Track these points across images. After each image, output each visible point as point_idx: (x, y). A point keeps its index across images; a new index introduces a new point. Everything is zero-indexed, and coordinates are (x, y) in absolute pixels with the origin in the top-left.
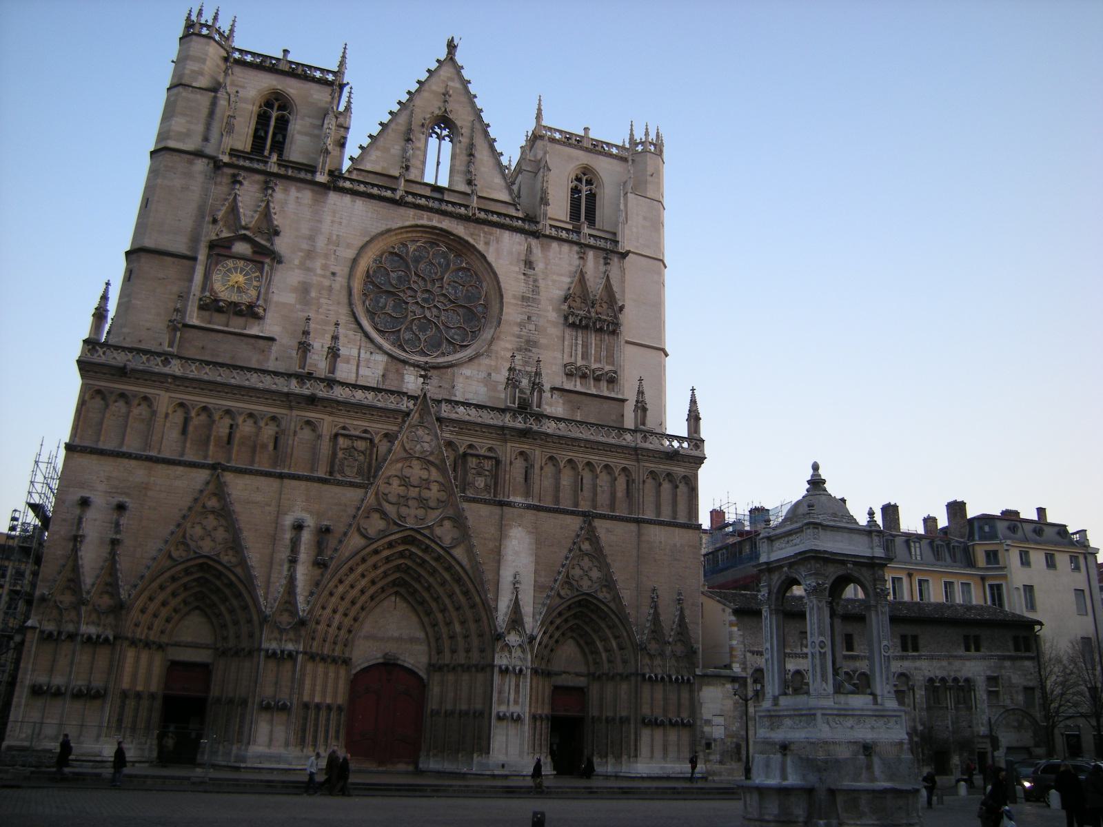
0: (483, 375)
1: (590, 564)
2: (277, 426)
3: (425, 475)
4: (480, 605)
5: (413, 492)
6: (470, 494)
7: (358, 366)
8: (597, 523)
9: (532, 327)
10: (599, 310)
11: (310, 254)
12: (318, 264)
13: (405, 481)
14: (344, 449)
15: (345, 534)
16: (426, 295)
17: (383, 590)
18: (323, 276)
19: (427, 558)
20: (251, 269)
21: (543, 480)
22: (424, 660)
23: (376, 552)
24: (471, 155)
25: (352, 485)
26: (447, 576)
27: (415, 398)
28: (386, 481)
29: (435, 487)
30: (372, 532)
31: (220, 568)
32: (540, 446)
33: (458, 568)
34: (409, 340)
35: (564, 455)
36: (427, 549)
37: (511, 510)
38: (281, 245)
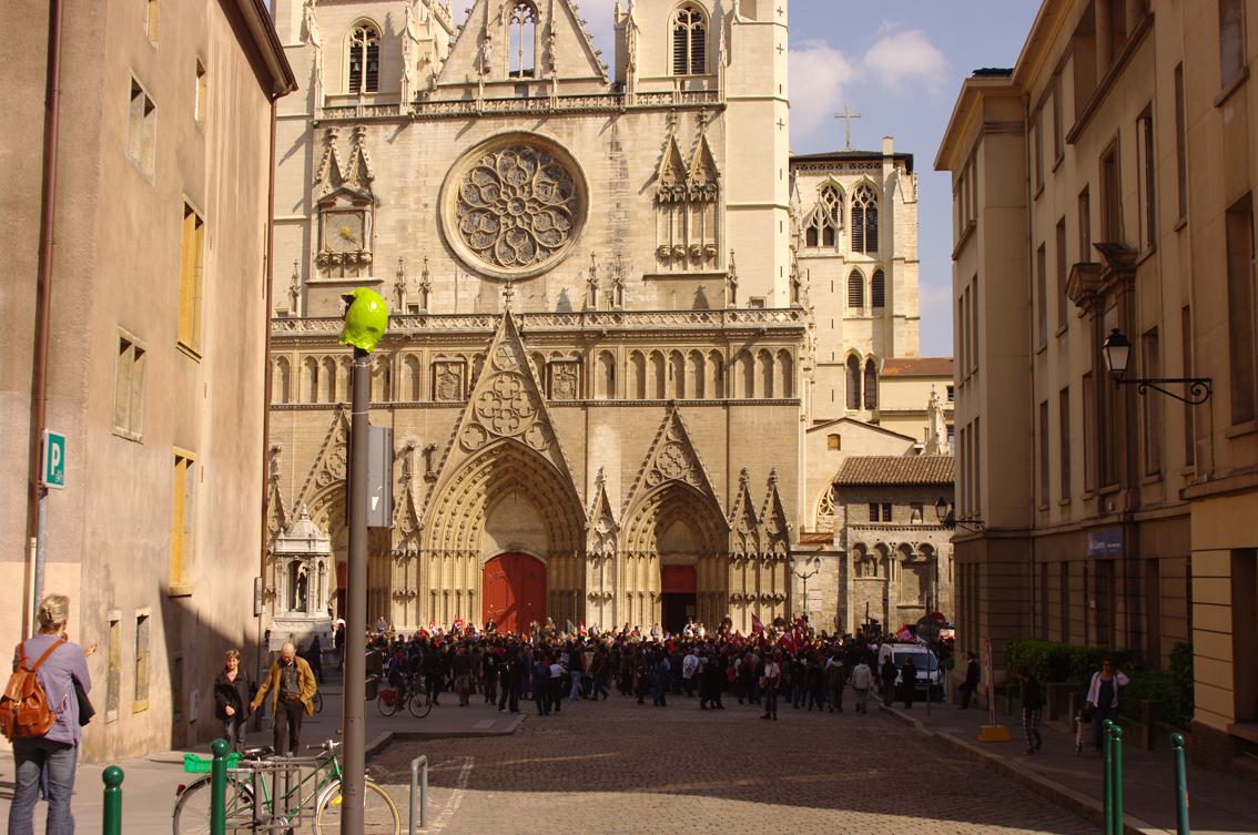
0: (574, 276)
1: (679, 452)
5: (506, 405)
7: (456, 291)
8: (682, 412)
9: (622, 215)
11: (403, 192)
12: (410, 200)
13: (497, 395)
15: (448, 450)
16: (516, 204)
17: (500, 490)
18: (417, 210)
22: (544, 548)
23: (479, 461)
24: (549, 33)
29: (524, 397)
30: (473, 446)
35: (647, 350)
37: (596, 409)
38: (378, 188)
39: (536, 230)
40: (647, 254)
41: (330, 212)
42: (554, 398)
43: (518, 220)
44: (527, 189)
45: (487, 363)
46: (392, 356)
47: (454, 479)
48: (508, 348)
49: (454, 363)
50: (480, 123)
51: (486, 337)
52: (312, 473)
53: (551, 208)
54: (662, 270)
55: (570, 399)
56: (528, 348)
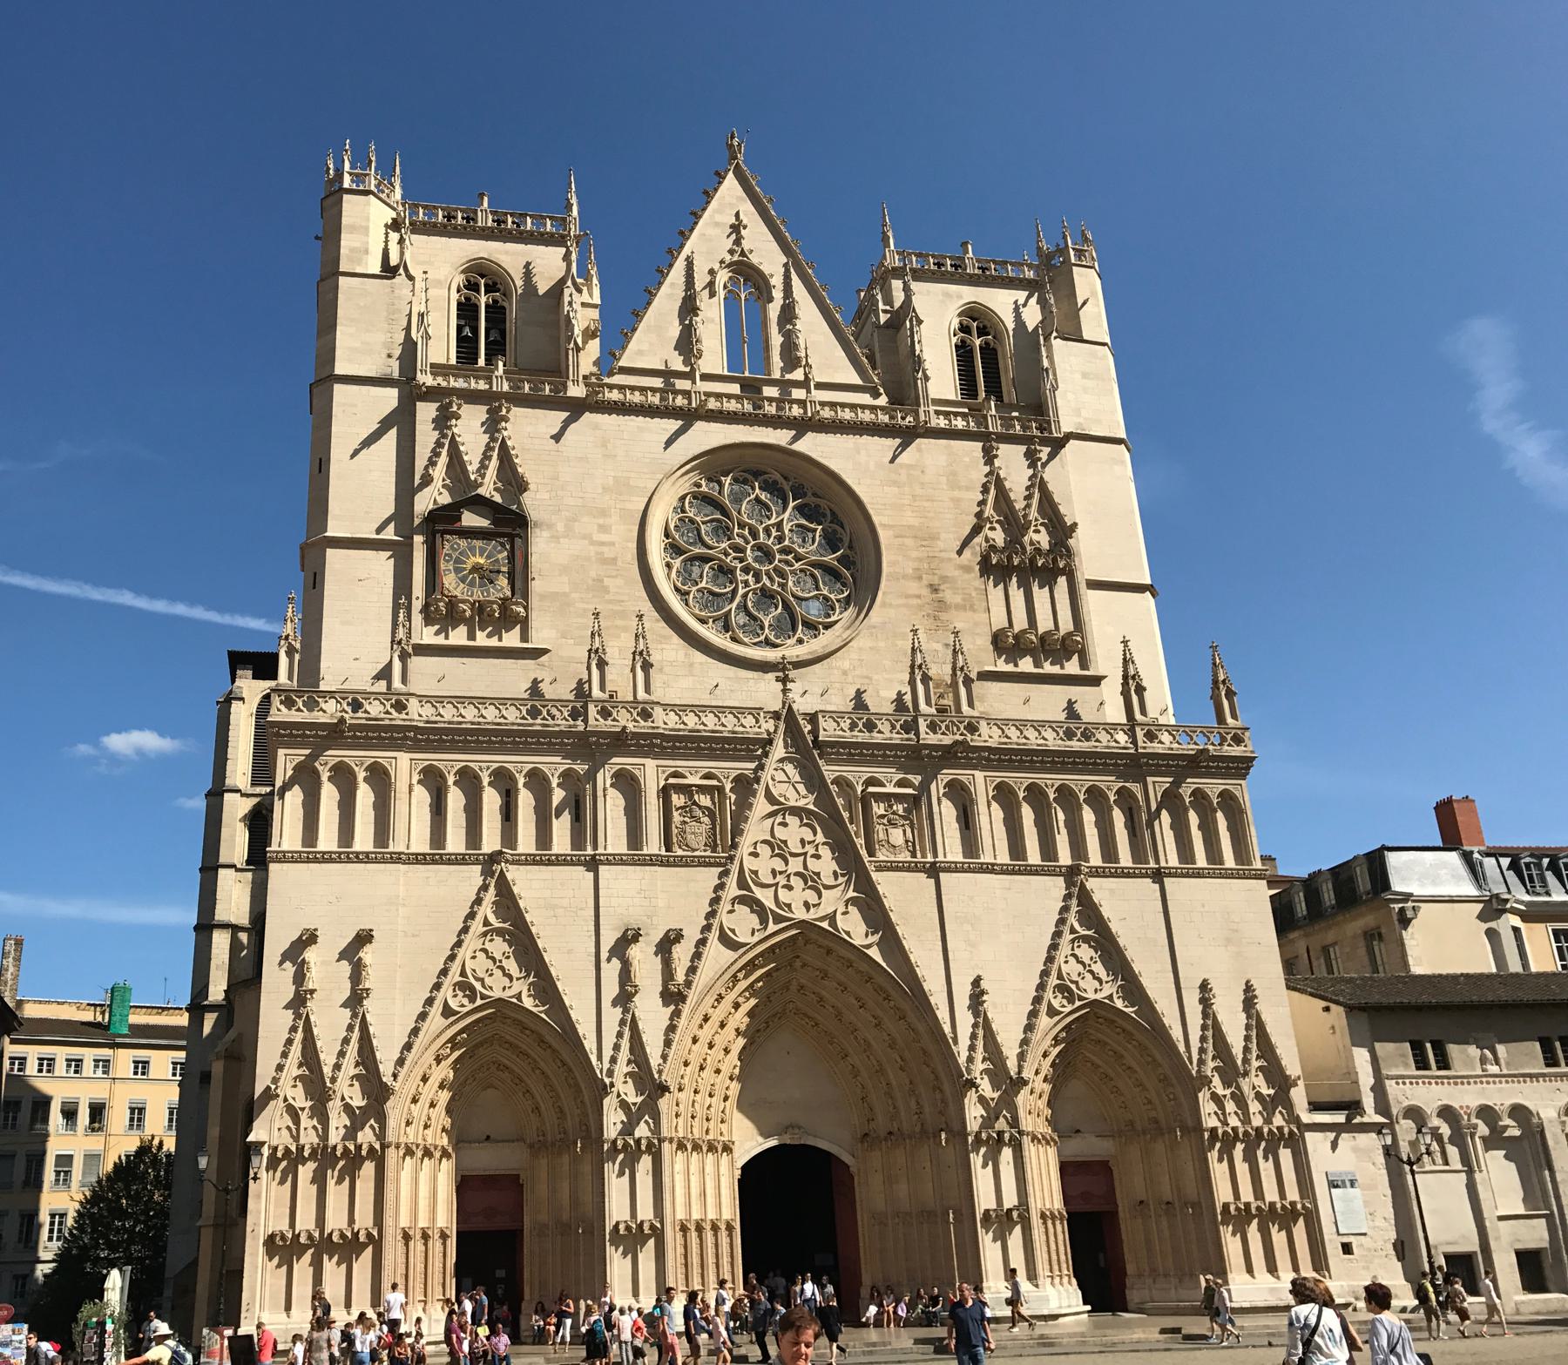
5: (795, 865)
6: (882, 855)
10: (1035, 537)
13: (778, 848)
20: (495, 548)
21: (990, 819)
25: (704, 863)
27: (776, 716)
28: (752, 850)
34: (744, 625)
38: (533, 503)
39: (793, 596)
40: (979, 641)
41: (451, 533)
42: (882, 855)
43: (765, 580)
44: (774, 533)
46: (591, 776)
47: (710, 1000)
48: (790, 768)
49: (702, 789)
50: (700, 426)
51: (755, 748)
52: (437, 986)
53: (815, 565)
54: (1003, 666)
55: (905, 856)
56: (830, 771)
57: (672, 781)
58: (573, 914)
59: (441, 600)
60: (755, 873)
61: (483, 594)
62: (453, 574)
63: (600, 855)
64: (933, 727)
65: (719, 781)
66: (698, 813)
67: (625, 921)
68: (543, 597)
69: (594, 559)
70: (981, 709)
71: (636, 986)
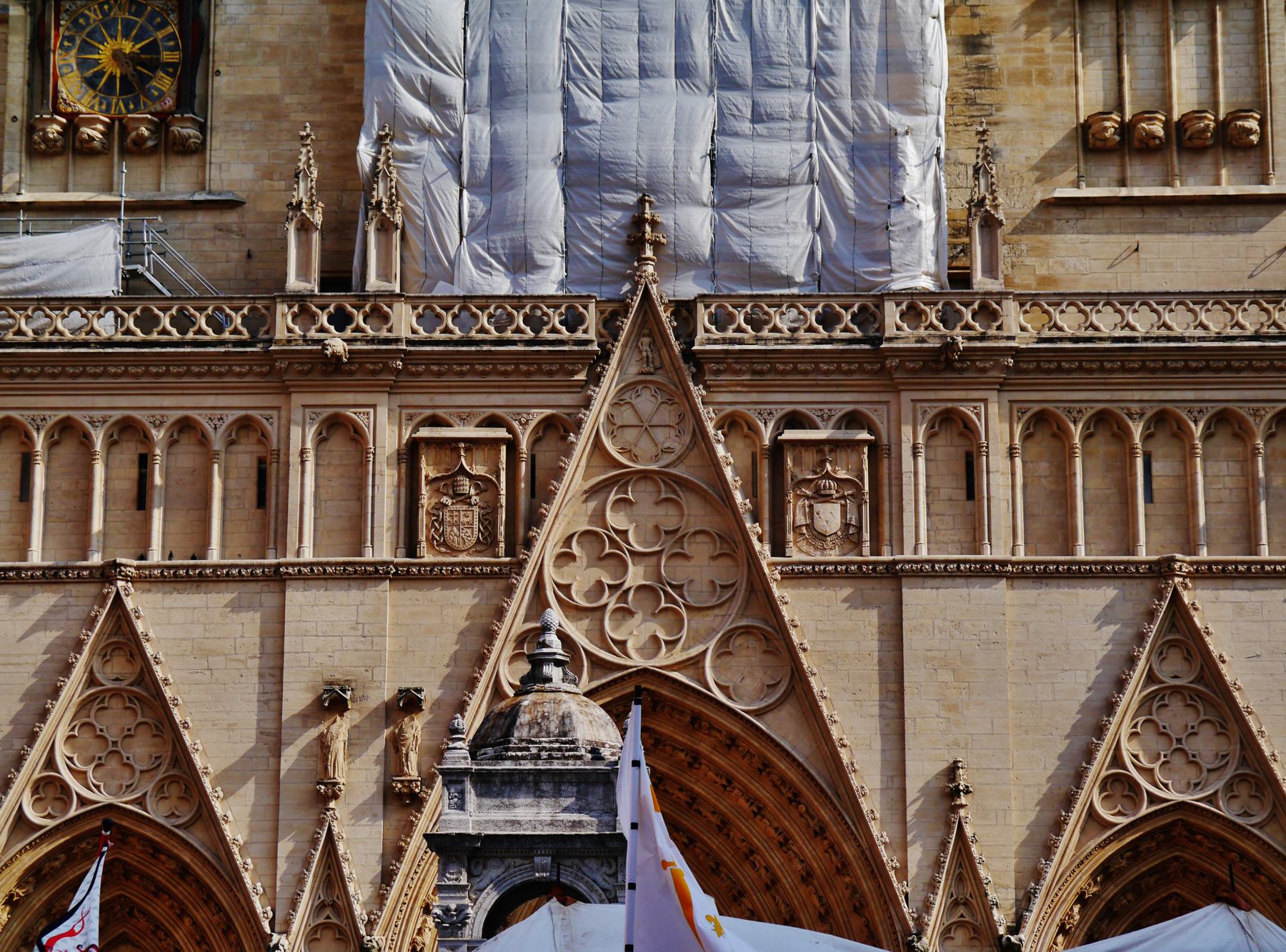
1: (1190, 718)
2: (260, 442)
3: (669, 519)
4: (857, 867)
6: (795, 554)
14: (436, 479)
19: (704, 748)
20: (150, 19)
26: (763, 792)
29: (700, 550)
31: (149, 833)
32: (1002, 387)
33: (782, 765)
36: (696, 721)
42: (795, 554)
45: (582, 443)
57: (425, 432)
58: (240, 665)
59: (53, 121)
60: (566, 588)
61: (126, 106)
62: (76, 72)
63: (287, 565)
64: (913, 314)
65: (510, 430)
66: (466, 486)
67: (327, 677)
68: (234, 106)
69: (326, 30)
70: (1042, 271)
71: (335, 784)
